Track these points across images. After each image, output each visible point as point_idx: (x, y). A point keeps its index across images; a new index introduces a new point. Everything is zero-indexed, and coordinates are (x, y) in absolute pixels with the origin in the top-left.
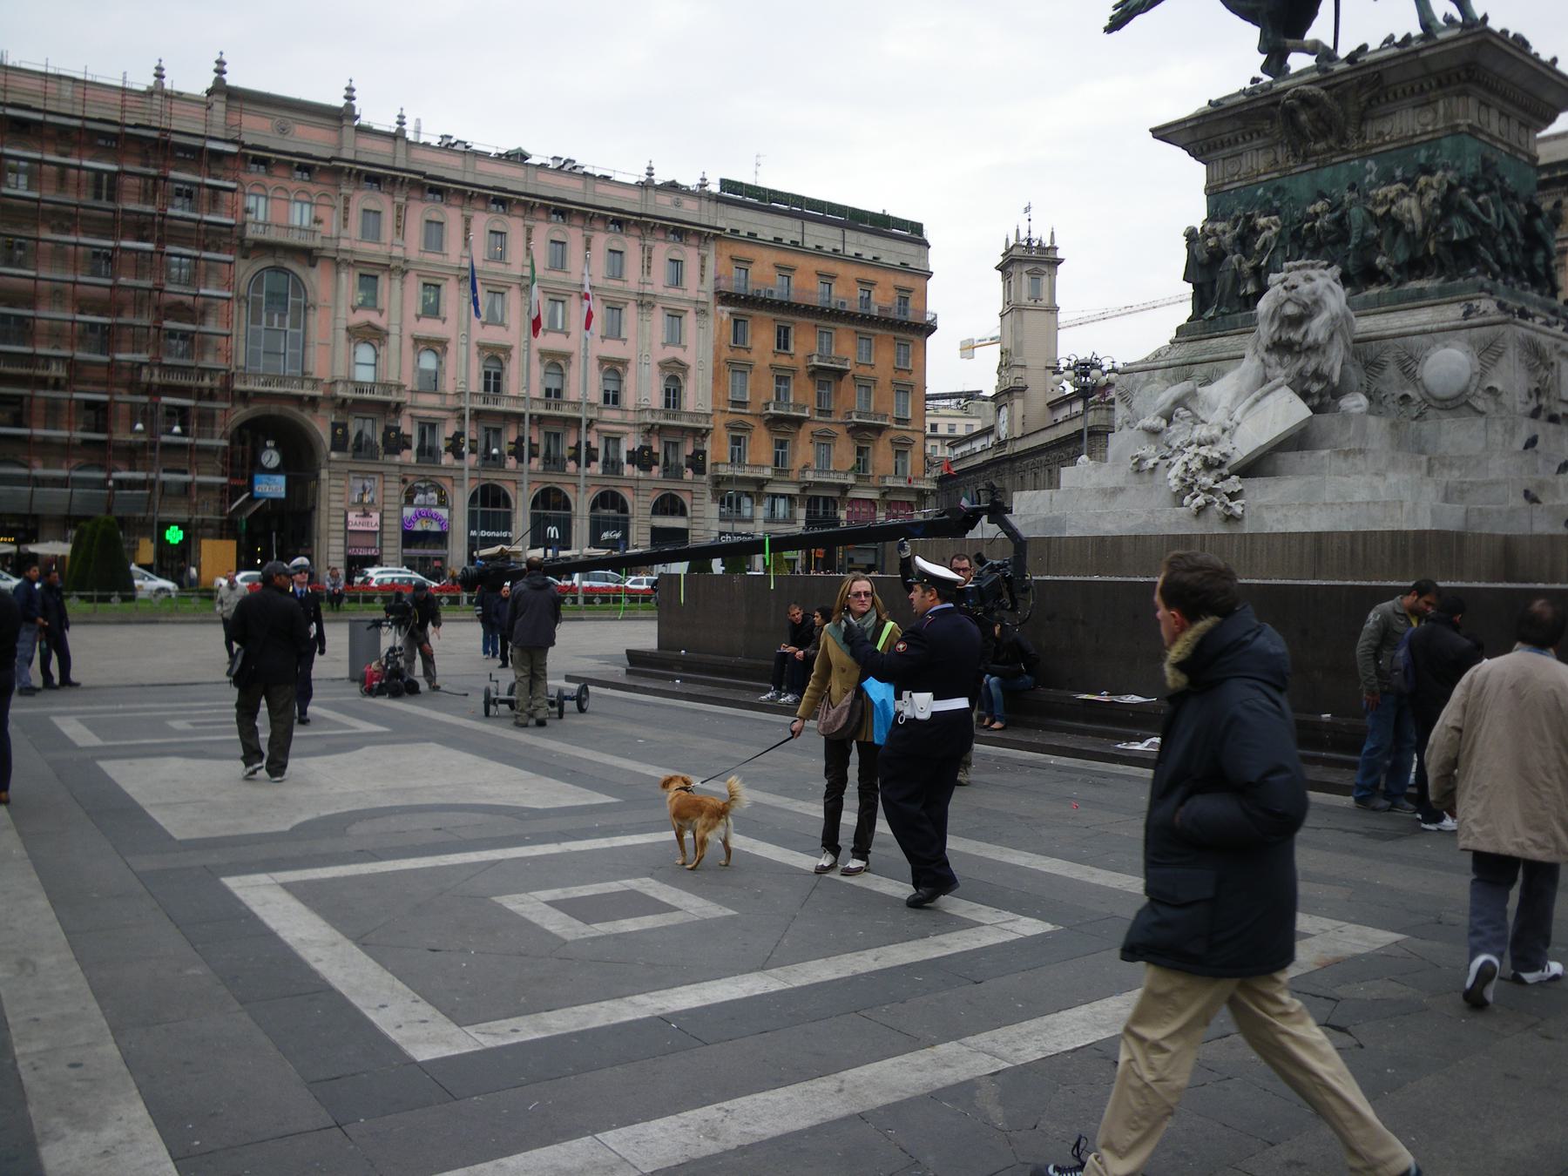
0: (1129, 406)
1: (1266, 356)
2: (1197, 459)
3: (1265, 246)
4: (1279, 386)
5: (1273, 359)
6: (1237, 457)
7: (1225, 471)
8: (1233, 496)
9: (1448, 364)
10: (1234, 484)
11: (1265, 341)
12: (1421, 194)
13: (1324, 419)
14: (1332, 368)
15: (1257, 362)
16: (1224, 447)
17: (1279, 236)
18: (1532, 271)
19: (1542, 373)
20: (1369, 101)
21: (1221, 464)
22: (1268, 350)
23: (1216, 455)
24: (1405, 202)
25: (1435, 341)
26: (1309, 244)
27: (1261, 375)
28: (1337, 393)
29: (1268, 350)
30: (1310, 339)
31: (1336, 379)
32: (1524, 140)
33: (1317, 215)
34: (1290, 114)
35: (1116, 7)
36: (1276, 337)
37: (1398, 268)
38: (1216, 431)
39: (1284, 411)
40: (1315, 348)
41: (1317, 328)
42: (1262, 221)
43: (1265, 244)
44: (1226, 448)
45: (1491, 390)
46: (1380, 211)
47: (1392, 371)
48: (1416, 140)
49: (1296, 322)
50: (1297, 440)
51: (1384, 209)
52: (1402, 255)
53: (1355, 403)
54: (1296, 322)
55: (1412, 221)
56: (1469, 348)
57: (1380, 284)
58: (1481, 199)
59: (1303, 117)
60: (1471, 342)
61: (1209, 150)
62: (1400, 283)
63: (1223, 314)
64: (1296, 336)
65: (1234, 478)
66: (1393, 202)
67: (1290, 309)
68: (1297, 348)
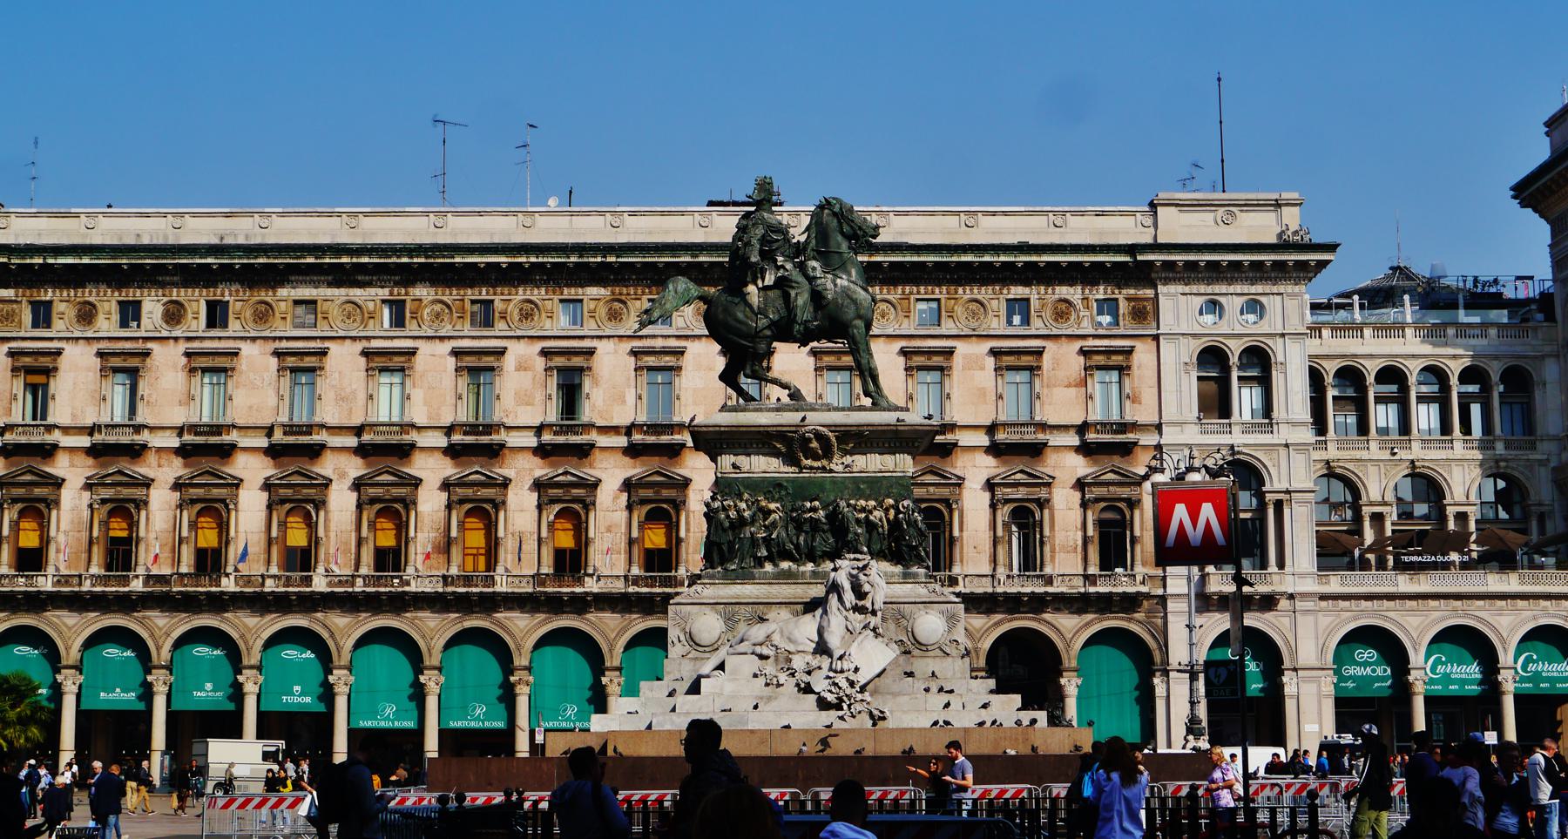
12: (887, 510)
24: (876, 513)
42: (773, 506)
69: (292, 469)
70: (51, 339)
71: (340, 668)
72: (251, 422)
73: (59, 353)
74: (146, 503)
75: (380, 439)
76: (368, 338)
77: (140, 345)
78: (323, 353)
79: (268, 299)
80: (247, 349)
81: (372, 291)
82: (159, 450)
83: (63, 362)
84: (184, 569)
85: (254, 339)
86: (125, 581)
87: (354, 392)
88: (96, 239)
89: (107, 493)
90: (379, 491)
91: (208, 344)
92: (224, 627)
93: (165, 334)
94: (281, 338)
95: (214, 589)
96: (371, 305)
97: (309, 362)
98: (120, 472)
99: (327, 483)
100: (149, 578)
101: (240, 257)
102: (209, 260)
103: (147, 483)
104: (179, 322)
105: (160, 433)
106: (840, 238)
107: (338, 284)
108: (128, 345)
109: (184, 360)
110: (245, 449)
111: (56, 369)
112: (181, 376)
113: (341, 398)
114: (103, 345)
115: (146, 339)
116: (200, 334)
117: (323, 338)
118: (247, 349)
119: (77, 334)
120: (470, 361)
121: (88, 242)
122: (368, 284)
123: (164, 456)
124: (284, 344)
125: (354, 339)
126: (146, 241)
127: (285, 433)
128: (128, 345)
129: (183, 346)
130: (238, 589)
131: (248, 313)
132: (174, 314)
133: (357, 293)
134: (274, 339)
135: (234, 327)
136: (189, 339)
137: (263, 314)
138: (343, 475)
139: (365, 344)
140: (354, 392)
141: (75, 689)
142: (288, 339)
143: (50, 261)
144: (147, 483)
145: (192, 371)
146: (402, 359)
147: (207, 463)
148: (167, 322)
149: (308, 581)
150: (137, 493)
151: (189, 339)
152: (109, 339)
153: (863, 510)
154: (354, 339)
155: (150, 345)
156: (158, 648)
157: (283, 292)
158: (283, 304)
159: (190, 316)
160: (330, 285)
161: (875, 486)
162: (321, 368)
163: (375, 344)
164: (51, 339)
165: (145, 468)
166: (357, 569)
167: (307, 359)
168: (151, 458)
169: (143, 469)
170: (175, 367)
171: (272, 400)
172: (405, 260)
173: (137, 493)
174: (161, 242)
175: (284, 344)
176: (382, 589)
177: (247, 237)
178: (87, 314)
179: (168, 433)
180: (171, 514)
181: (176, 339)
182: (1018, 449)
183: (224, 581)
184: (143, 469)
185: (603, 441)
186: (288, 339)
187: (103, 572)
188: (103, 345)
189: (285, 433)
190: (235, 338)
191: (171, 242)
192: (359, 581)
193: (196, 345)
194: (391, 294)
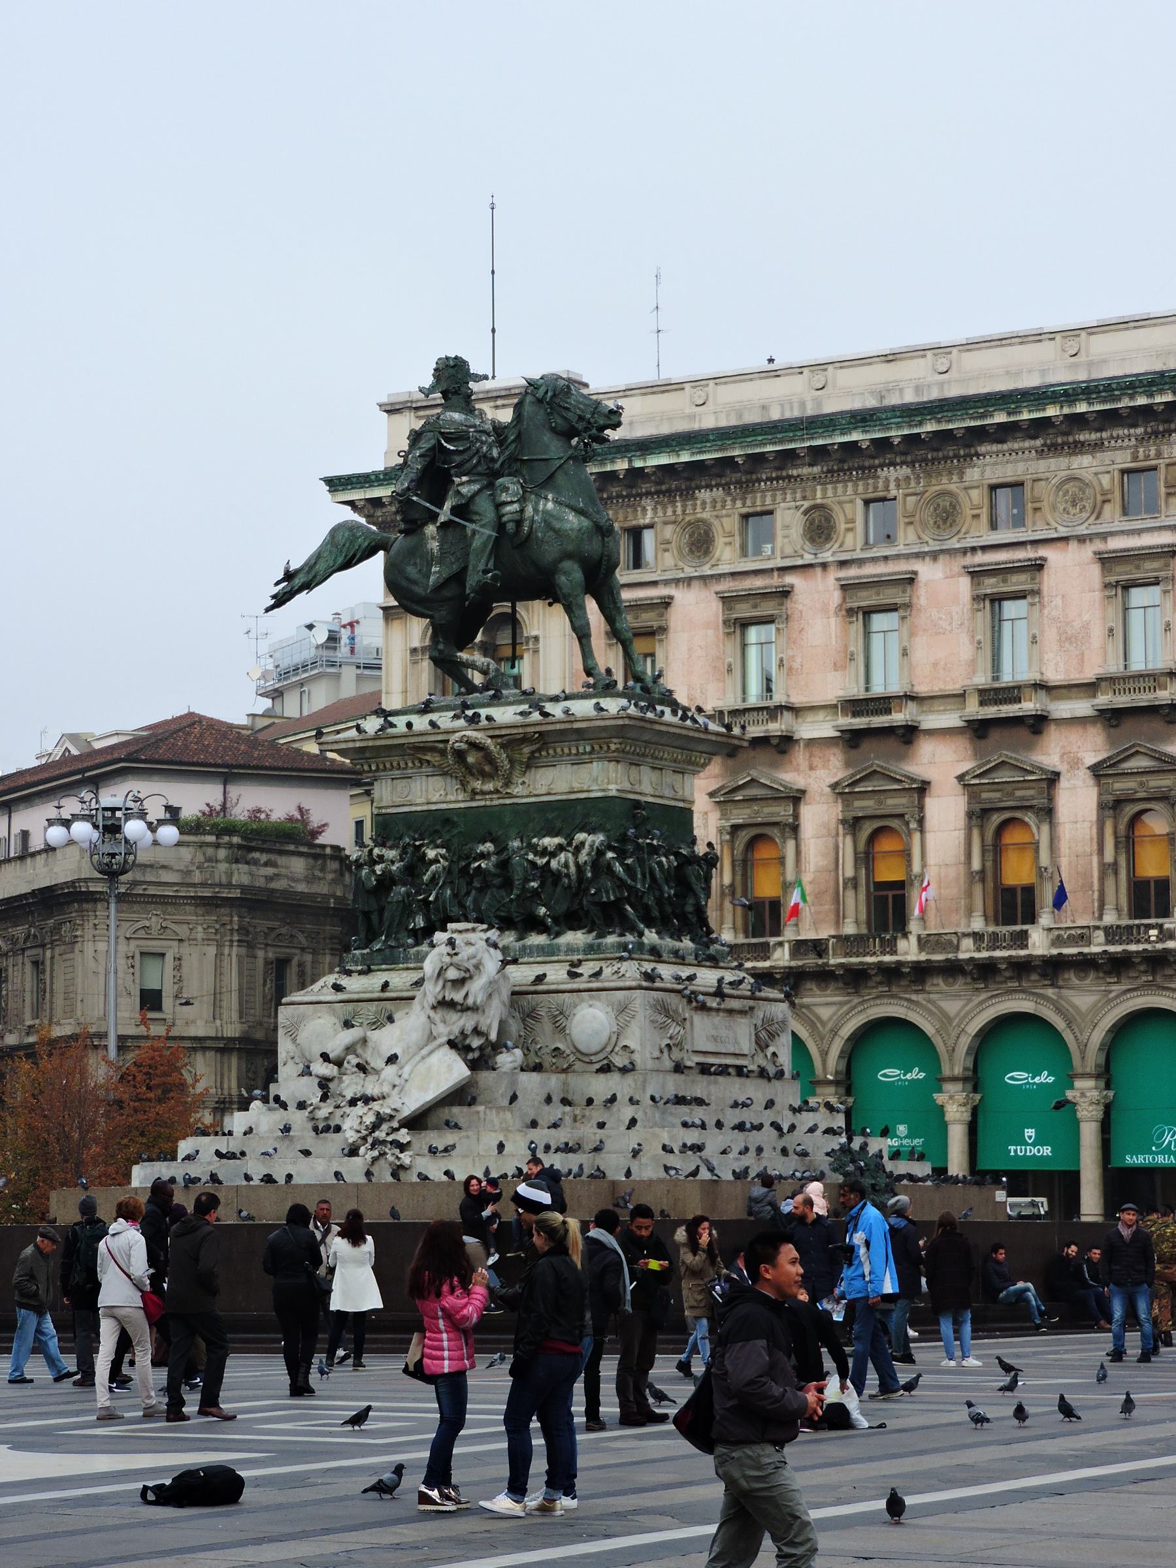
0: (294, 1040)
1: (432, 1013)
2: (371, 1113)
3: (434, 879)
4: (440, 1046)
5: (437, 1016)
6: (406, 1112)
7: (395, 1125)
8: (403, 1147)
9: (591, 1021)
10: (403, 1136)
11: (431, 1000)
13: (485, 1077)
14: (490, 1026)
15: (423, 1019)
16: (394, 1102)
17: (448, 871)
18: (683, 917)
19: (674, 1029)
20: (533, 753)
21: (392, 1117)
22: (434, 1008)
23: (388, 1111)
25: (582, 1001)
26: (476, 884)
27: (427, 1032)
28: (498, 1046)
29: (434, 1008)
30: (470, 1001)
31: (493, 1036)
32: (678, 787)
33: (483, 856)
34: (460, 755)
35: (277, 584)
36: (440, 997)
37: (556, 920)
38: (386, 1089)
39: (450, 1070)
40: (474, 1009)
41: (476, 990)
43: (434, 875)
44: (397, 1105)
45: (625, 1046)
46: (541, 861)
47: (547, 1026)
48: (573, 796)
49: (459, 983)
50: (461, 1096)
51: (545, 860)
52: (561, 908)
53: (508, 1060)
54: (459, 983)
55: (568, 875)
56: (609, 1009)
57: (540, 932)
58: (629, 861)
59: (471, 759)
60: (611, 1004)
61: (378, 770)
62: (558, 935)
63: (391, 947)
64: (458, 997)
65: (404, 1131)
66: (553, 855)
67: (452, 974)
68: (459, 1007)
69: (995, 759)
70: (654, 583)
71: (1084, 1076)
72: (937, 688)
73: (666, 603)
74: (795, 829)
75: (1123, 701)
76: (1104, 536)
77: (774, 581)
78: (1038, 566)
79: (953, 487)
80: (927, 571)
81: (1107, 456)
82: (811, 742)
83: (675, 617)
84: (850, 929)
85: (935, 555)
86: (763, 951)
87: (1086, 626)
88: (708, 421)
89: (740, 816)
90: (1128, 784)
91: (870, 570)
92: (914, 1017)
93: (808, 558)
94: (974, 549)
95: (887, 958)
96: (1105, 480)
97: (1018, 582)
98: (753, 782)
99: (1053, 779)
100: (799, 947)
101: (899, 426)
102: (855, 436)
103: (796, 798)
104: (828, 538)
105: (810, 717)
106: (547, 437)
107: (1053, 449)
108: (758, 583)
109: (836, 596)
110: (931, 732)
111: (663, 630)
112: (834, 623)
113: (1067, 639)
114: (726, 586)
115: (783, 570)
116: (858, 554)
117: (1035, 543)
118: (927, 571)
119: (689, 571)
120: (991, 585)
121: (696, 426)
122: (1098, 446)
123: (817, 751)
124: (981, 558)
125: (1082, 539)
126: (775, 415)
127: (982, 703)
128: (758, 583)
129: (834, 574)
130: (923, 957)
131: (928, 514)
132: (820, 528)
133: (1084, 463)
134: (964, 551)
135: (907, 539)
136: (843, 564)
137: (946, 515)
138: (1075, 763)
139: (1098, 545)
140: (1086, 626)
141: (1097, 1113)
142: (984, 548)
143: (638, 464)
144: (796, 798)
145: (851, 612)
146: (1156, 564)
147: (874, 756)
148: (812, 540)
149: (1021, 939)
150: (783, 812)
151: (843, 564)
152: (733, 574)
153: (544, 852)
154: (1082, 539)
155: (790, 579)
156: (824, 1054)
157: (973, 474)
158: (975, 493)
159: (842, 526)
160: (1041, 453)
161: (567, 815)
162: (1036, 592)
163: (1115, 544)
164: (654, 583)
165: (792, 774)
166: (1100, 918)
167: (1015, 578)
168: (800, 756)
169: (791, 776)
170: (825, 610)
171: (965, 650)
172: (1142, 401)
173: (783, 812)
174: (796, 413)
175: (981, 558)
176: (1133, 948)
177: (918, 389)
178: (700, 542)
179: (821, 715)
180: (831, 841)
181: (824, 566)
182: (1004, 724)
183: (902, 944)
184: (791, 776)
185: (1063, 708)
186: (984, 548)
187: (741, 940)
188: (726, 586)
189: (982, 703)
190: (908, 557)
191: (810, 412)
192: (1100, 936)
193: (852, 572)
194: (1135, 458)
